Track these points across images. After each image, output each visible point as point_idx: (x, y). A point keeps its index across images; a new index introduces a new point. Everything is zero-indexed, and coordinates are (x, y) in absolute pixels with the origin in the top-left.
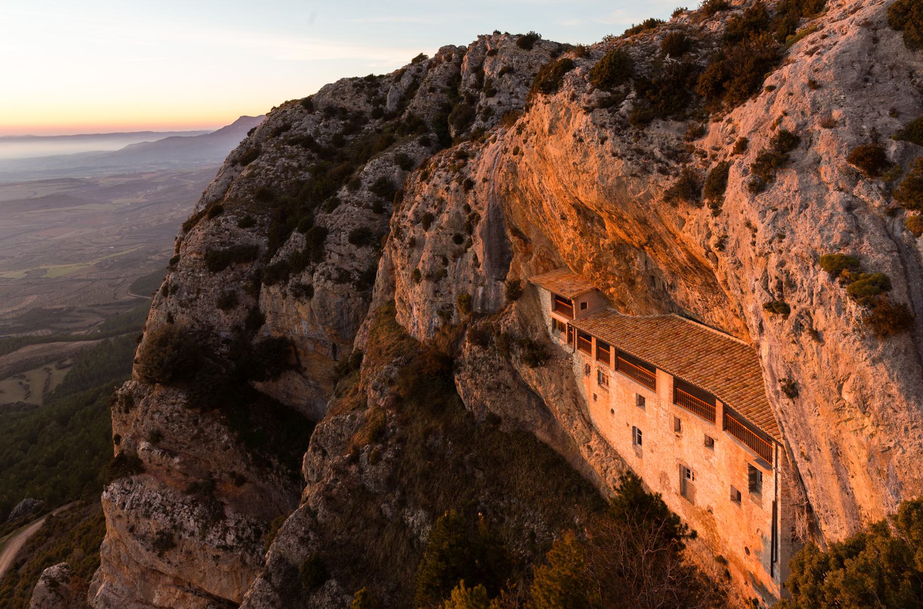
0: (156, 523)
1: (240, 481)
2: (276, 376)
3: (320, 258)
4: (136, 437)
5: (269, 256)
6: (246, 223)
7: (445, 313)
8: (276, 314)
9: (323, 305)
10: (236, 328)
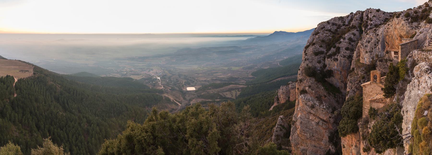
0: (310, 103)
1: (325, 97)
2: (330, 77)
3: (339, 53)
4: (305, 87)
5: (327, 53)
6: (321, 46)
7: (373, 58)
8: (329, 65)
9: (340, 62)
10: (321, 67)
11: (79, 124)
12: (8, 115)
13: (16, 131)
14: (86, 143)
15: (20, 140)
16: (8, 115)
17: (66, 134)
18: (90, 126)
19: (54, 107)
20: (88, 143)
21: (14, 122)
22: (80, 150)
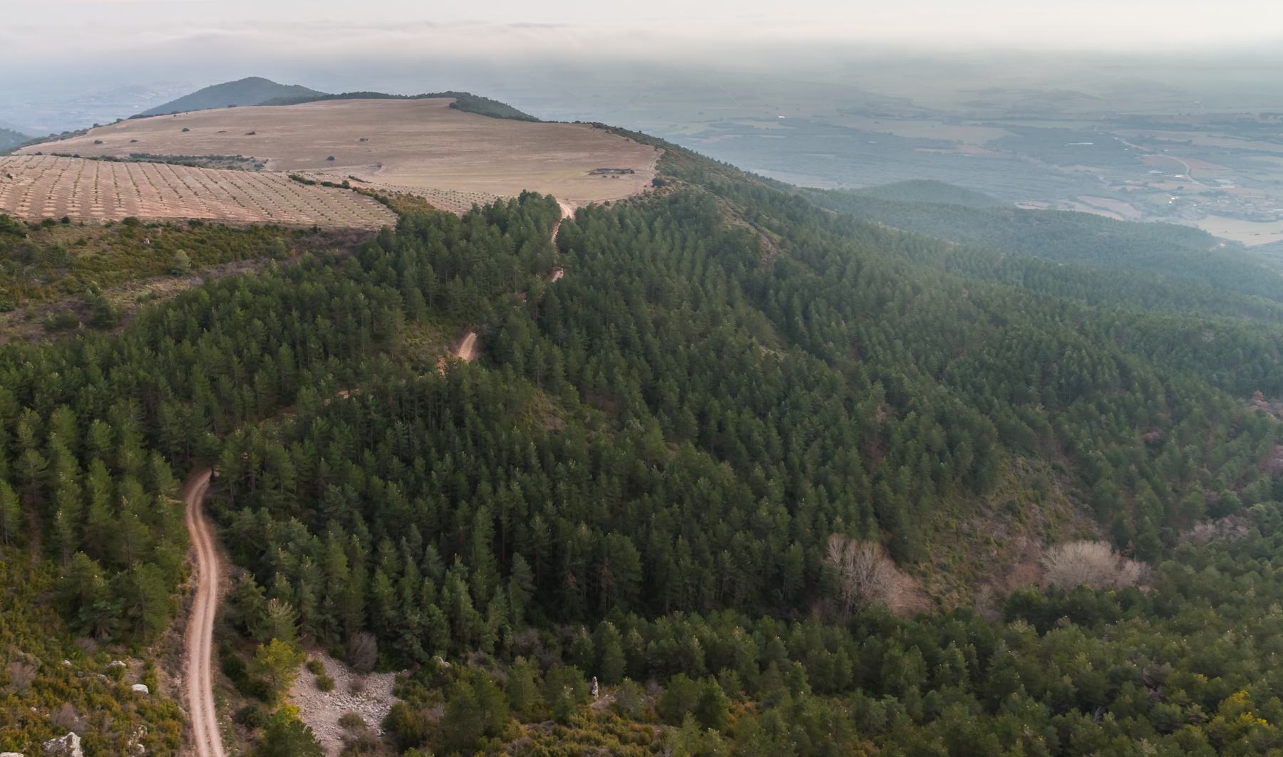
11: (849, 402)
12: (518, 355)
13: (554, 414)
14: (866, 480)
15: (568, 442)
16: (518, 355)
17: (774, 433)
18: (902, 417)
19: (739, 325)
20: (877, 479)
21: (548, 382)
22: (832, 501)
